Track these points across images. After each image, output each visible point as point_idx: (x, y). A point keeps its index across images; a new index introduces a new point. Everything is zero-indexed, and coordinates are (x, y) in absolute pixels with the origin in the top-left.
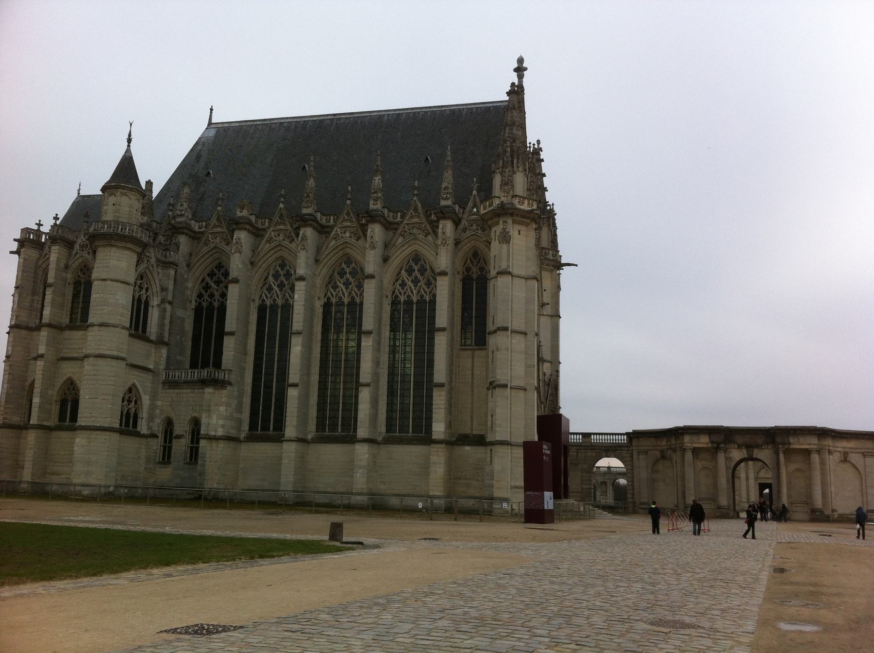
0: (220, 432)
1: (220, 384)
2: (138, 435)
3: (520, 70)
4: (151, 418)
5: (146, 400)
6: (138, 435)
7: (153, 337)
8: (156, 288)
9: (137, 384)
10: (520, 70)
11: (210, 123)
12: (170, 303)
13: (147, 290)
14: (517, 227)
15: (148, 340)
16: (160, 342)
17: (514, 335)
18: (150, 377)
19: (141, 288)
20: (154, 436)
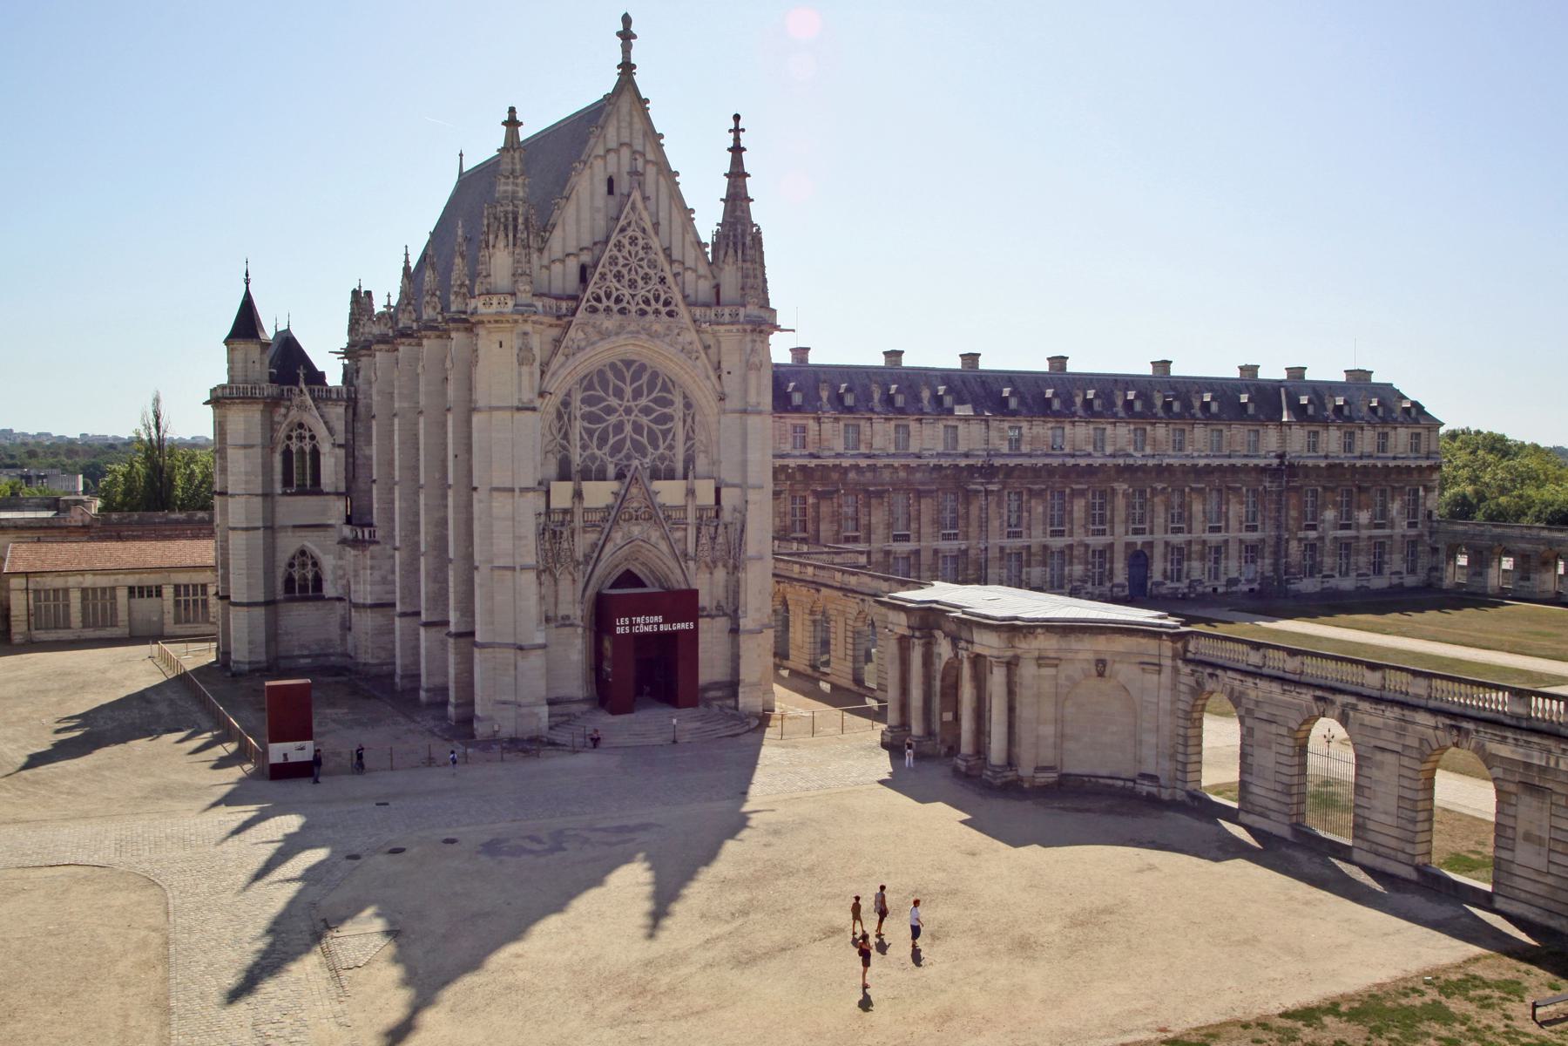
0: (369, 601)
1: (356, 543)
2: (322, 598)
3: (626, 36)
4: (334, 583)
5: (328, 563)
6: (322, 598)
7: (327, 489)
8: (321, 431)
9: (308, 544)
10: (626, 36)
11: (461, 174)
12: (340, 446)
13: (313, 437)
14: (496, 337)
15: (320, 493)
16: (337, 494)
17: (495, 494)
18: (331, 532)
19: (301, 438)
20: (340, 599)
